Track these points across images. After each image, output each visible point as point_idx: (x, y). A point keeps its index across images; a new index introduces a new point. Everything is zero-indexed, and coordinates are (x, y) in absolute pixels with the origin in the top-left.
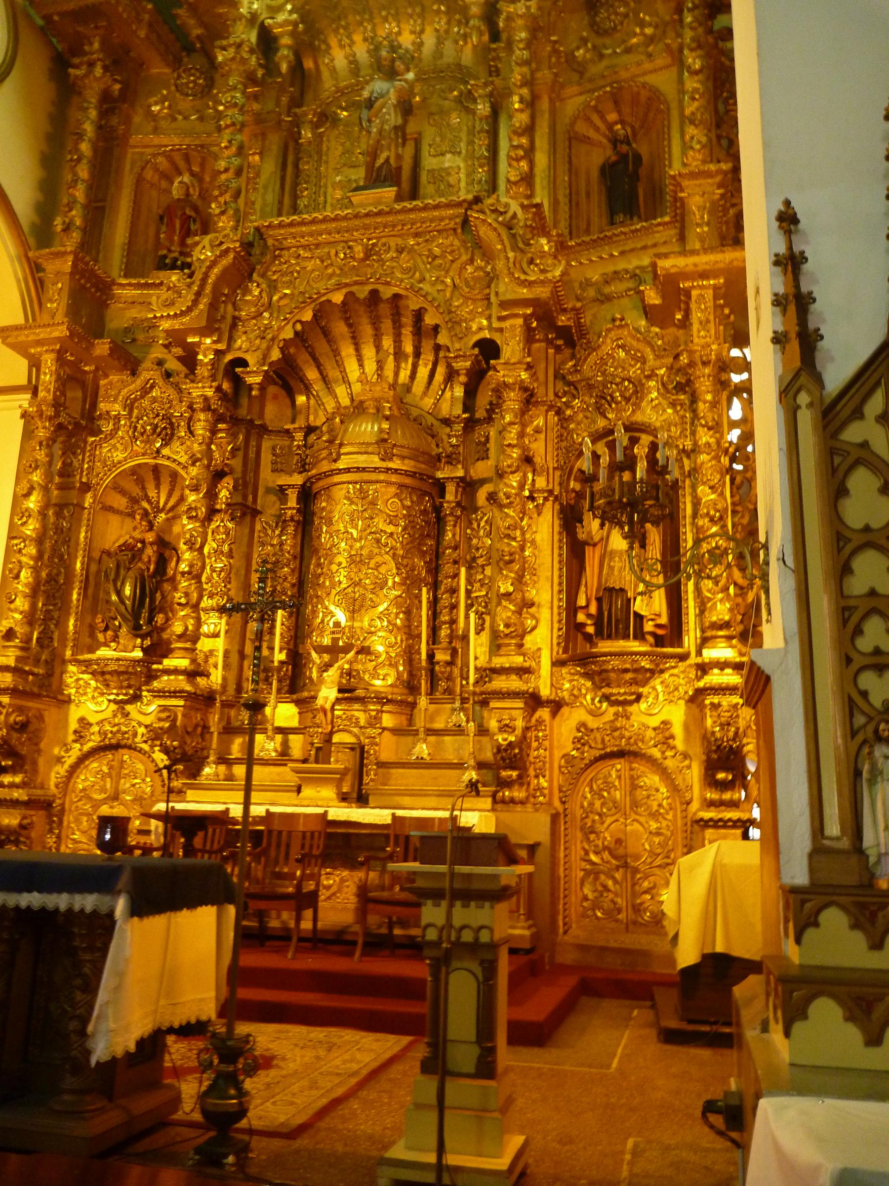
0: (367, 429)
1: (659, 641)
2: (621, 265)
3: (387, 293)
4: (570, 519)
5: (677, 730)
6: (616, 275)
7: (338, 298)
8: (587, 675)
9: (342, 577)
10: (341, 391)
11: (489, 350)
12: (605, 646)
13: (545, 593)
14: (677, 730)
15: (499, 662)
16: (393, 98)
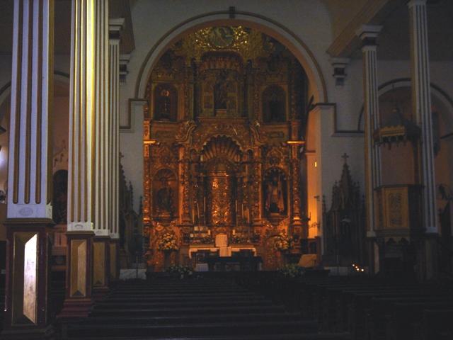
0: (221, 166)
1: (282, 213)
2: (277, 130)
3: (228, 136)
4: (265, 188)
5: (286, 231)
6: (275, 133)
7: (216, 136)
8: (268, 220)
9: (219, 200)
10: (211, 153)
11: (251, 152)
12: (272, 214)
13: (260, 203)
14: (286, 231)
15: (255, 219)
16: (225, 85)
